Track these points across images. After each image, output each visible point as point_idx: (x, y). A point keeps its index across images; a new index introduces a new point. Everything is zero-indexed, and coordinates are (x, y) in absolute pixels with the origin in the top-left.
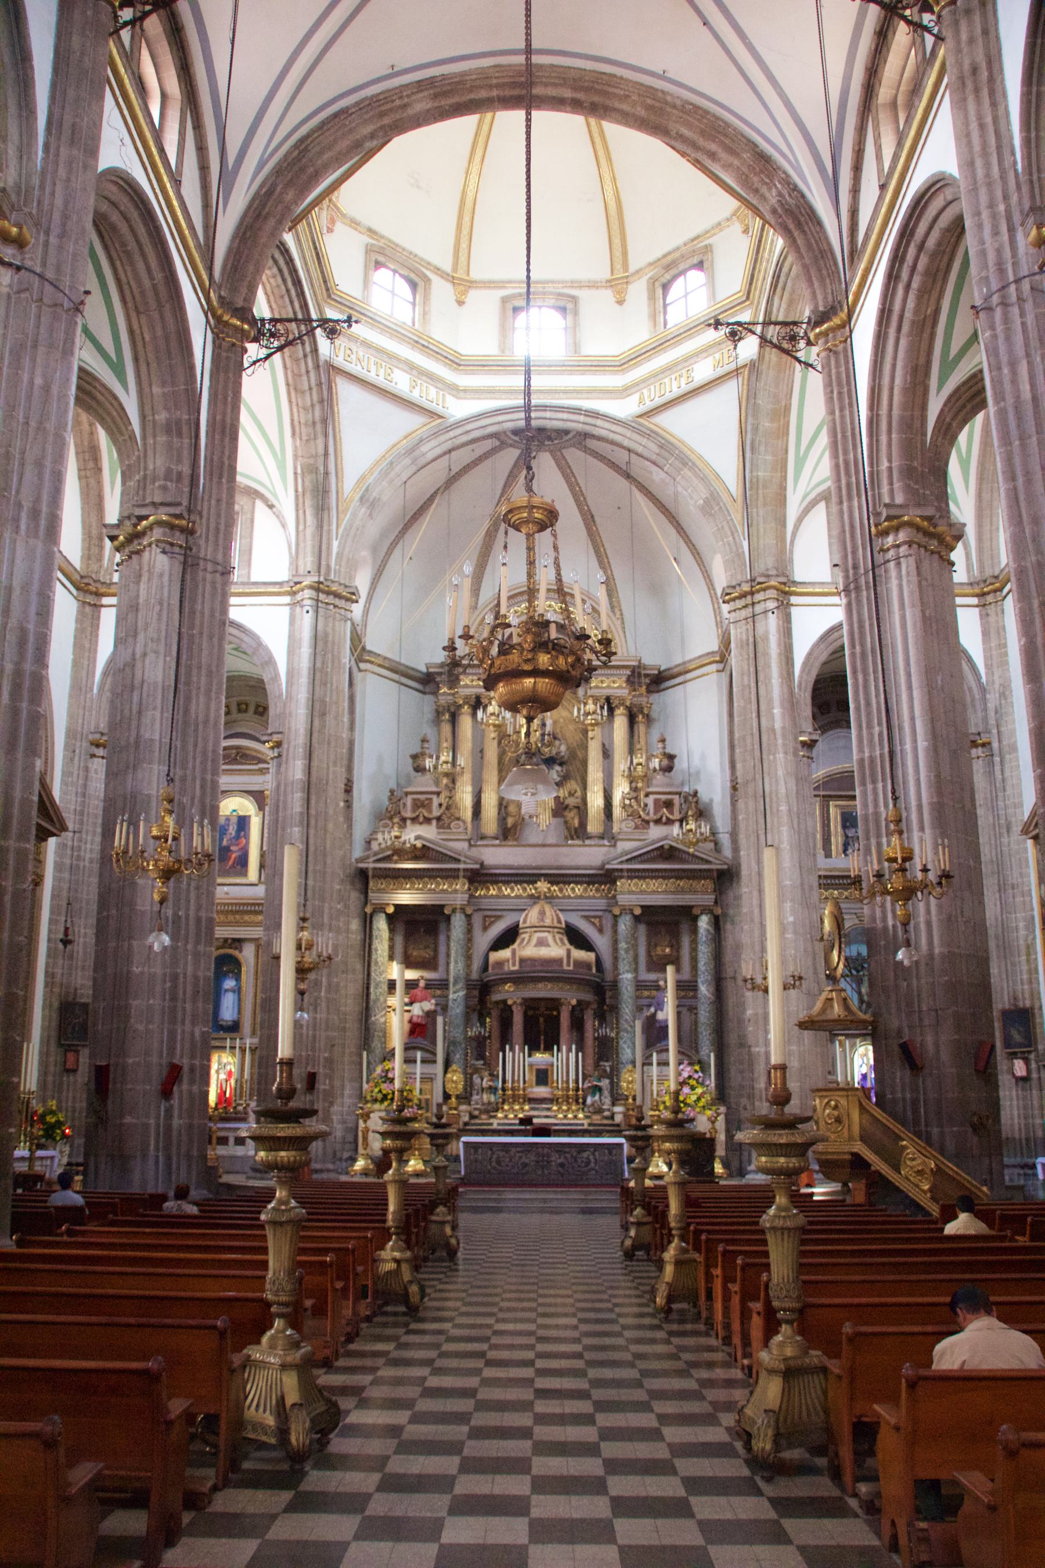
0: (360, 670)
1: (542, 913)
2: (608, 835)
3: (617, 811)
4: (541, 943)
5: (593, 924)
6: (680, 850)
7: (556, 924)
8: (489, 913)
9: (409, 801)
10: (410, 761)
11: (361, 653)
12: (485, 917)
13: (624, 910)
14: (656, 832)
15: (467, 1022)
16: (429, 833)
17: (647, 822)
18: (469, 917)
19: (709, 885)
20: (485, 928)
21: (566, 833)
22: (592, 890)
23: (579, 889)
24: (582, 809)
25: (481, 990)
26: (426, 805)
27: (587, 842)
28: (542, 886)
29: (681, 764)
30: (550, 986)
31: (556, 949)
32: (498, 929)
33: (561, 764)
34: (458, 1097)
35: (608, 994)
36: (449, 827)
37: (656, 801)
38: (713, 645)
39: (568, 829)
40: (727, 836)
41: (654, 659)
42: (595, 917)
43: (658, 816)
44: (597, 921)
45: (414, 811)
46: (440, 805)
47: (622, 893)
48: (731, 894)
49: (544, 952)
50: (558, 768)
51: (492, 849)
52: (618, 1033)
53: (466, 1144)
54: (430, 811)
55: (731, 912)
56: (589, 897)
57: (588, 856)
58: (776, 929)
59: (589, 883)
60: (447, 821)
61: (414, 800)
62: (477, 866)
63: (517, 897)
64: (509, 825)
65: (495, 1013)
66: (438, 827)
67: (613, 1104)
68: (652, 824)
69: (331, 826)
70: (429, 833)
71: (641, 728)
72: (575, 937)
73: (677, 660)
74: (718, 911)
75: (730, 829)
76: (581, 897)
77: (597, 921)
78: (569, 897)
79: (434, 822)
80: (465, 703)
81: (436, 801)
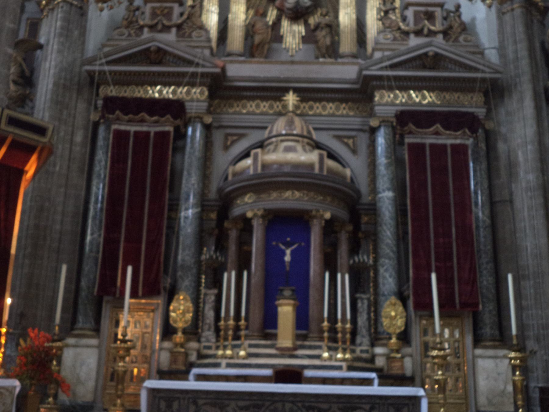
1: (291, 123)
4: (288, 150)
5: (347, 144)
6: (446, 57)
7: (305, 133)
8: (229, 131)
12: (227, 135)
13: (384, 122)
15: (200, 241)
17: (406, 34)
18: (207, 128)
19: (478, 98)
20: (226, 148)
23: (331, 107)
24: (333, 28)
27: (340, 60)
28: (291, 99)
30: (297, 194)
34: (184, 331)
35: (365, 219)
36: (190, 36)
37: (416, 14)
39: (319, 48)
40: (494, 52)
42: (349, 137)
43: (419, 27)
44: (350, 142)
46: (182, 14)
47: (380, 105)
48: (502, 111)
49: (291, 157)
52: (376, 260)
53: (153, 392)
54: (170, 19)
55: (503, 130)
56: (342, 116)
59: (341, 101)
60: (188, 31)
62: (218, 70)
63: (262, 114)
65: (233, 234)
66: (178, 35)
67: (373, 345)
68: (412, 36)
70: (169, 39)
74: (490, 125)
75: (496, 44)
76: (333, 115)
77: (350, 142)
78: (320, 115)
79: (174, 30)
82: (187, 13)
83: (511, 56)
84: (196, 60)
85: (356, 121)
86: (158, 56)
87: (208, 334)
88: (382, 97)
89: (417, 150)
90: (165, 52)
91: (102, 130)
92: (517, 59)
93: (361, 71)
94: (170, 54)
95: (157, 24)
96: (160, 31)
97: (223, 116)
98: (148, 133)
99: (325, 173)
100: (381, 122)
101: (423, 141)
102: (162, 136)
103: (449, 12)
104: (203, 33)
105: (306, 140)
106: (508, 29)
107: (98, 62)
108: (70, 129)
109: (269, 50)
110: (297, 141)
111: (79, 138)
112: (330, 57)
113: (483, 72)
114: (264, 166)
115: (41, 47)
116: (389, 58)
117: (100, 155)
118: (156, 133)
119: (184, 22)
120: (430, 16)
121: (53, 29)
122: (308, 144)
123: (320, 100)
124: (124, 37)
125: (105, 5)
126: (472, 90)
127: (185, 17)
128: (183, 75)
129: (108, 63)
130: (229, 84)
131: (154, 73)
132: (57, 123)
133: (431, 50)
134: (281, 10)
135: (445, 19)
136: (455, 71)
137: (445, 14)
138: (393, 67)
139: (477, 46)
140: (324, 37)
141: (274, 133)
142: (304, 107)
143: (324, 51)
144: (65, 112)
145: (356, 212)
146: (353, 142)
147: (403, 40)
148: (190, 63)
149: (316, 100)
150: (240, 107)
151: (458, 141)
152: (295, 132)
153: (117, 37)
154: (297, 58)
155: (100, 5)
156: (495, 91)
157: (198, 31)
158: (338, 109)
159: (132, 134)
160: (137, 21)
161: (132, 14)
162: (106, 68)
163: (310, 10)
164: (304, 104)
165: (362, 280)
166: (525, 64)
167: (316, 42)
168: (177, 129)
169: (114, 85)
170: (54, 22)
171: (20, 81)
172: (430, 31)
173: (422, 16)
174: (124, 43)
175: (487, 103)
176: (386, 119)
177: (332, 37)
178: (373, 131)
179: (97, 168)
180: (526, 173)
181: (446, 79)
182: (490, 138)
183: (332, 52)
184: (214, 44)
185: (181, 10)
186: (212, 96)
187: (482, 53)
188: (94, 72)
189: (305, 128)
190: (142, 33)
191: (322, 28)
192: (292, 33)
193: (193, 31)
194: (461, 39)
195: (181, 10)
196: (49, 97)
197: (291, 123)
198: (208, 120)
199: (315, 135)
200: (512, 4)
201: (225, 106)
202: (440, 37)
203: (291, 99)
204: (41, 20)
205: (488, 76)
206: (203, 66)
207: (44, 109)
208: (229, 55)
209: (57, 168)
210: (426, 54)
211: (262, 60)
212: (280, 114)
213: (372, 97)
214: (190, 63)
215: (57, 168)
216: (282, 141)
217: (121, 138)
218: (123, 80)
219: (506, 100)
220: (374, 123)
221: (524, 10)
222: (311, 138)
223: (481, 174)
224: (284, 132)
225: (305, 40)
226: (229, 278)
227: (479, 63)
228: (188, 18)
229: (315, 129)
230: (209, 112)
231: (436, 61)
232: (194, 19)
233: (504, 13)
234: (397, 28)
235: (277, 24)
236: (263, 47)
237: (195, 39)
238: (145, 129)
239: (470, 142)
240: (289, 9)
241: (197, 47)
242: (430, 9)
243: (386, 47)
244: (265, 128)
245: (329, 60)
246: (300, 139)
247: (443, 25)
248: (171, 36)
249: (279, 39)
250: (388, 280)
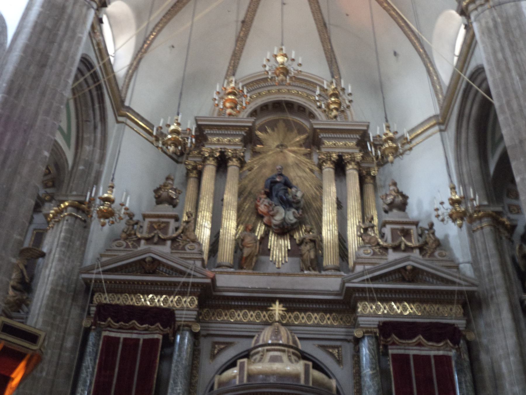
0: (118, 122)
1: (277, 333)
4: (274, 360)
5: (332, 354)
6: (423, 271)
7: (291, 343)
9: (146, 224)
10: (154, 194)
13: (368, 332)
17: (386, 249)
18: (195, 336)
19: (457, 310)
20: (213, 356)
21: (302, 265)
22: (328, 319)
23: (315, 317)
24: (317, 243)
26: (165, 228)
27: (323, 273)
28: (277, 309)
33: (297, 209)
36: (183, 248)
37: (393, 231)
39: (303, 261)
40: (468, 266)
42: (334, 347)
43: (396, 243)
44: (335, 352)
45: (150, 232)
46: (177, 229)
48: (482, 323)
49: (277, 367)
50: (293, 210)
51: (227, 276)
54: (166, 233)
55: (485, 341)
56: (327, 326)
59: (326, 311)
61: (151, 223)
62: (208, 281)
64: (245, 255)
66: (172, 248)
68: (390, 251)
69: (25, 170)
71: (369, 189)
74: (471, 336)
75: (470, 258)
76: (318, 325)
77: (335, 352)
78: (305, 325)
79: (169, 243)
80: (211, 155)
81: (173, 224)
82: (182, 228)
83: (485, 270)
84: (188, 271)
85: (340, 332)
86: (152, 266)
88: (364, 308)
89: (401, 361)
90: (159, 262)
92: (490, 273)
93: (343, 283)
94: (164, 264)
95: (153, 237)
96: (156, 244)
97: (210, 325)
98: (138, 340)
99: (311, 384)
100: (364, 333)
101: (407, 352)
102: (151, 343)
103: (423, 230)
104: (196, 245)
105: (291, 350)
106: (480, 245)
107: (95, 271)
108: (62, 334)
109: (257, 262)
110: (284, 351)
111: (69, 344)
112: (314, 269)
113: (460, 284)
114: (250, 376)
115: (43, 255)
116: (370, 272)
117: (88, 361)
118: (144, 340)
119: (179, 235)
120: (406, 234)
121: (56, 240)
122: (294, 354)
123: (305, 310)
124: (121, 248)
125: (107, 221)
126: (450, 302)
127: (180, 231)
128: (175, 284)
129: (105, 272)
130: (219, 294)
131: (147, 282)
132: (49, 328)
133: (409, 264)
134: (268, 226)
135: (420, 235)
136: (432, 284)
137: (420, 232)
138: (374, 279)
139: (452, 261)
140: (309, 251)
141: (261, 342)
142: (290, 317)
143: (309, 264)
144: (58, 318)
146: (338, 353)
147: (382, 254)
148: (182, 273)
149: (301, 310)
150: (228, 316)
151: (441, 353)
152: (281, 342)
153: (116, 248)
154: (282, 270)
155: (102, 220)
156: (472, 302)
157: (192, 244)
158: (322, 319)
159: (121, 340)
160: (135, 234)
161: (131, 227)
162: (102, 277)
163: (295, 227)
164: (290, 314)
166: (498, 277)
167: (301, 256)
168: (165, 337)
169: (108, 293)
170: (58, 233)
171: (19, 286)
172: (406, 246)
173: (399, 232)
174: (122, 254)
175: (466, 314)
176: (369, 330)
177: (316, 251)
178: (357, 341)
179: (83, 375)
180: (512, 385)
181: (424, 291)
182: (472, 349)
183: (316, 264)
184: (205, 256)
185: (177, 224)
186: (201, 305)
187: (457, 267)
188: (91, 280)
189: (290, 337)
190: (139, 245)
191: (306, 243)
192: (279, 247)
193: (186, 244)
194: (436, 254)
195: (177, 224)
196: (45, 302)
197: (277, 333)
198: (197, 328)
199: (300, 345)
200: (481, 222)
201: (213, 314)
202: (417, 251)
203: (277, 309)
204: (46, 230)
205: (464, 288)
206: (194, 277)
207: (38, 314)
208: (219, 266)
209: (44, 374)
210: (404, 268)
211: (250, 271)
212: (267, 324)
213: (355, 308)
214: (182, 273)
215: (44, 374)
216: (268, 350)
217: (110, 344)
218: (116, 288)
219: (484, 312)
220: (358, 333)
221: (492, 228)
222: (297, 349)
223: (466, 386)
224: (270, 342)
225: (290, 253)
227: (456, 277)
228: (182, 232)
229: (300, 339)
230: (198, 320)
231: (414, 274)
232: (188, 233)
233: (474, 231)
234: (376, 243)
235: (265, 238)
236: (252, 259)
237: (188, 251)
238: (134, 336)
239: (452, 353)
240: (276, 225)
241: (190, 259)
242: (406, 227)
243: (366, 261)
244: (252, 337)
245: (313, 272)
246: (286, 349)
247: (419, 241)
248: (166, 249)
249: (267, 252)
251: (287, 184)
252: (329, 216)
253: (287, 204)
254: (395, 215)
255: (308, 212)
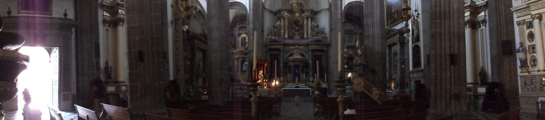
2: (307, 38)
3: (309, 34)
11: (264, 8)
14: (315, 37)
15: (283, 69)
16: (277, 38)
24: (303, 34)
25: (286, 63)
29: (320, 27)
31: (299, 57)
32: (289, 53)
38: (327, 7)
41: (315, 9)
57: (304, 42)
58: (338, 54)
70: (277, 38)
72: (302, 55)
73: (319, 9)
87: (285, 82)
89: (315, 55)
91: (268, 53)
145: (306, 63)
165: (307, 74)
183: (303, 38)
192: (297, 37)
217: (271, 54)
226: (288, 75)
250: (311, 74)
251: (298, 21)
252: (305, 28)
253: (298, 26)
254: (316, 29)
255: (302, 27)
